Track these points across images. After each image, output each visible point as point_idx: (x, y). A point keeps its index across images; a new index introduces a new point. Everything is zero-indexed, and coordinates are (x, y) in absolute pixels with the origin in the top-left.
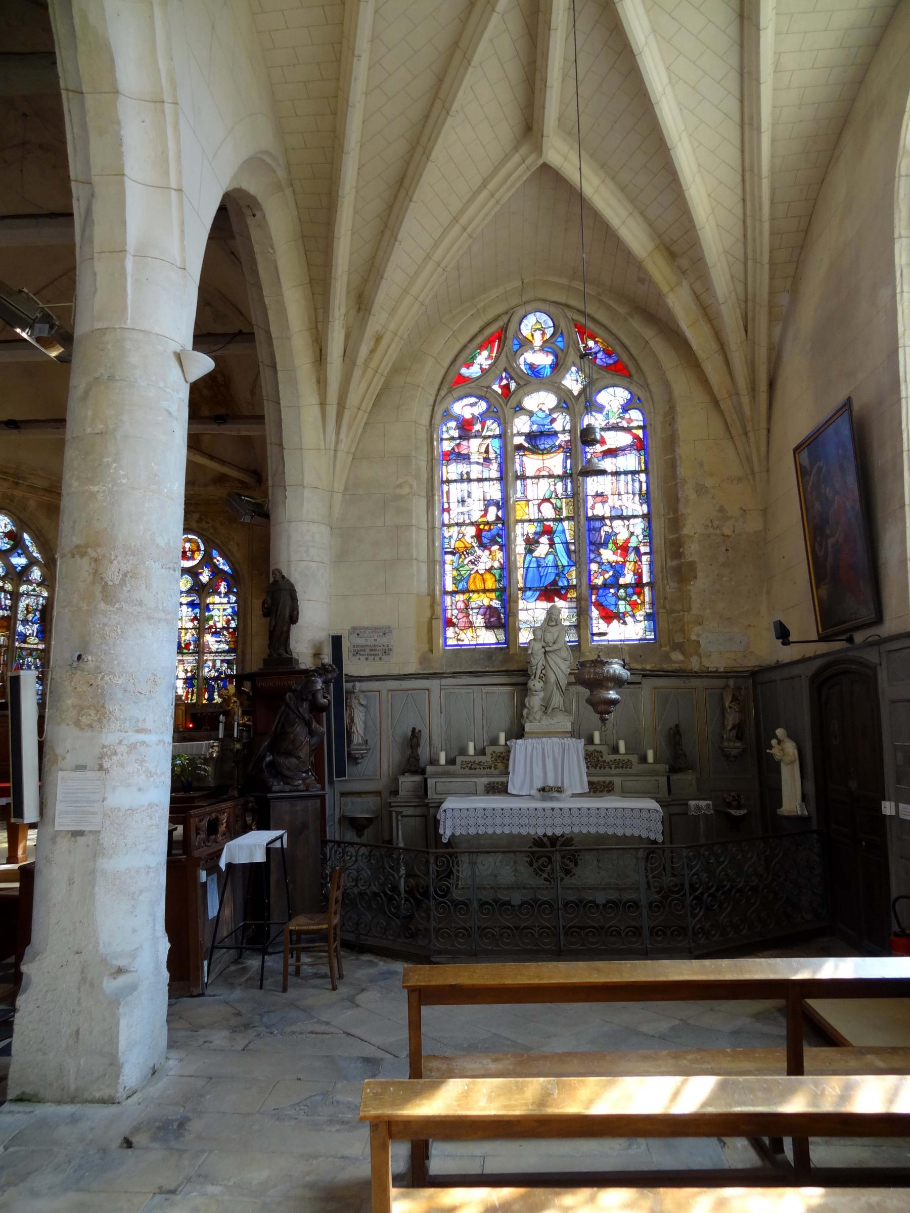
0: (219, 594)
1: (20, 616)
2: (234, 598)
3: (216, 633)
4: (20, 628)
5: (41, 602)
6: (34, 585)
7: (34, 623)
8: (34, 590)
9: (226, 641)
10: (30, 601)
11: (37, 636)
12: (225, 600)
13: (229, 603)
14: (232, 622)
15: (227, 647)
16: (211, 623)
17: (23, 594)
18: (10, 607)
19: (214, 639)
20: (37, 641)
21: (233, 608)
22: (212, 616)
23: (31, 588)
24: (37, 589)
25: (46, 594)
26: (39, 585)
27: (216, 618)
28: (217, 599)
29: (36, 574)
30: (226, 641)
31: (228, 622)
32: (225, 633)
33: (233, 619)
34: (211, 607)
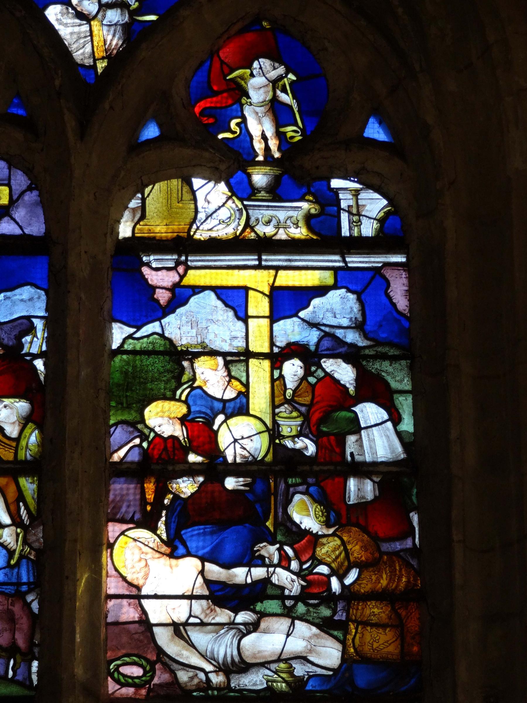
0: (232, 163)
2: (375, 204)
3: (226, 516)
9: (314, 592)
12: (289, 219)
13: (325, 237)
14: (370, 412)
15: (329, 654)
16: (163, 418)
19: (186, 574)
21: (366, 286)
22: (177, 358)
27: (211, 377)
28: (214, 206)
30: (314, 592)
31: (326, 412)
32: (305, 516)
33: (373, 388)
34: (159, 274)
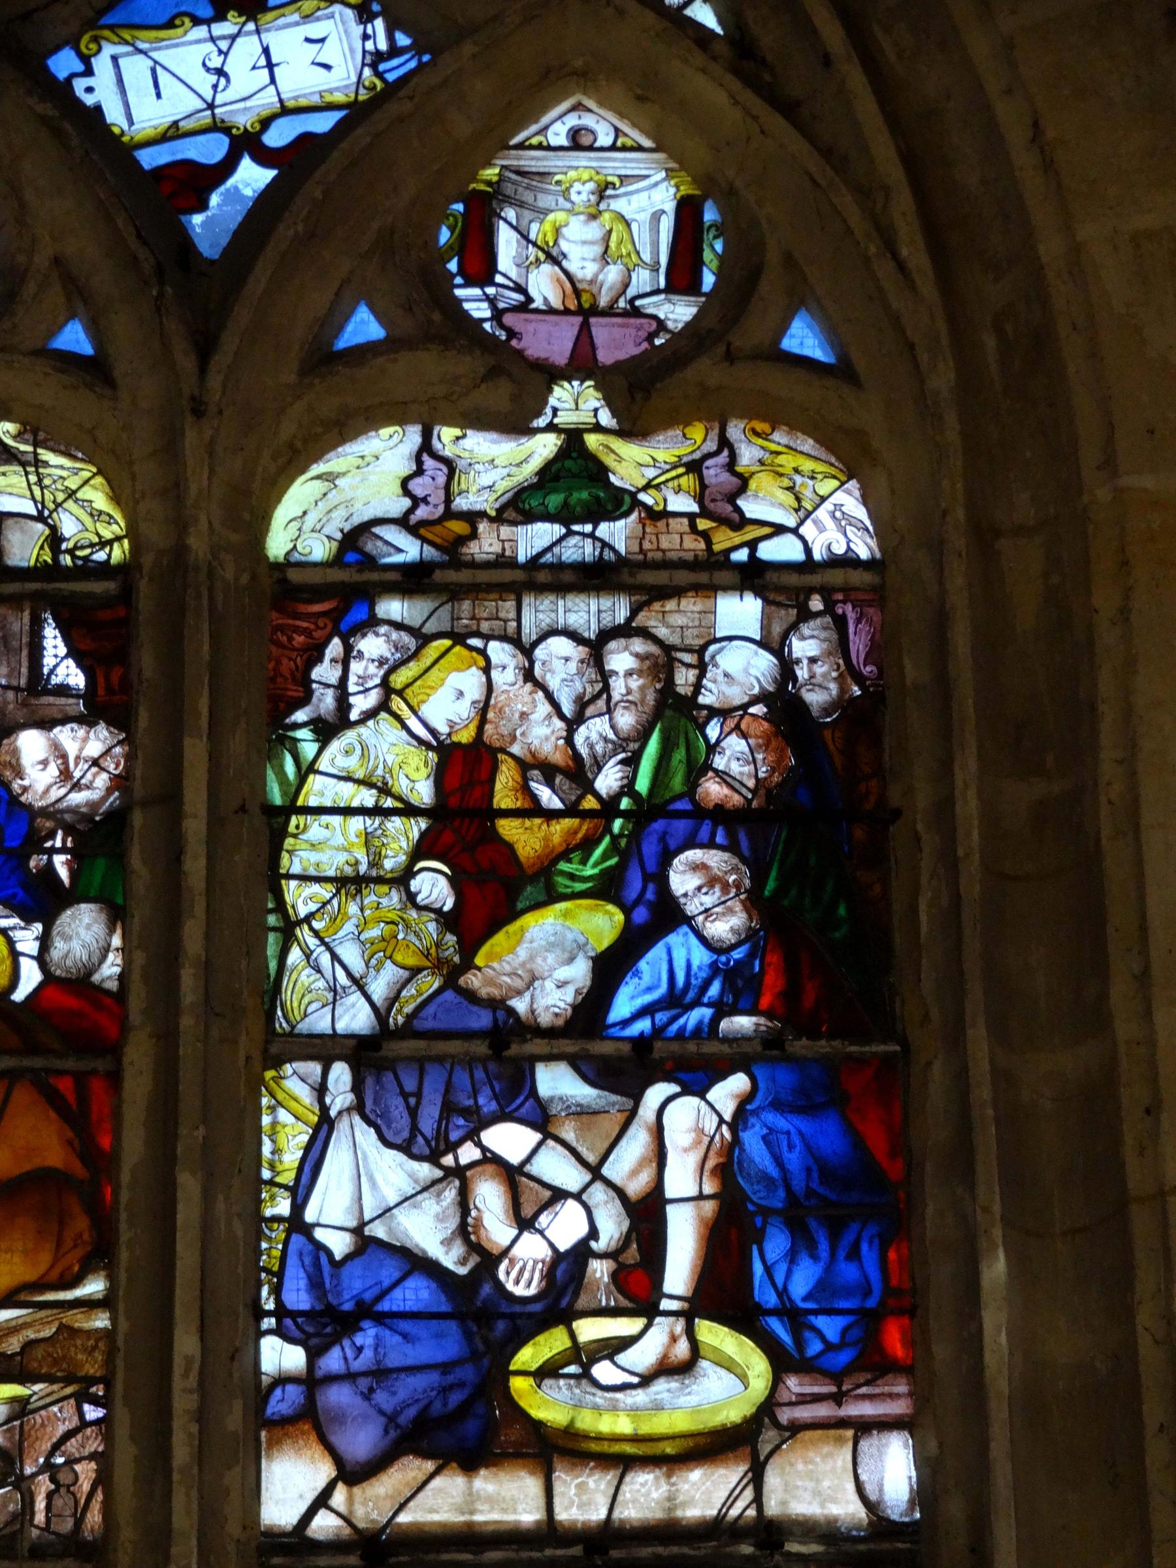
1: (339, 976)
4: (362, 1186)
5: (741, 670)
6: (575, 402)
7: (625, 1070)
8: (574, 483)
10: (539, 688)
11: (723, 1294)
17: (351, 583)
18: (97, 835)
20: (731, 1379)
23: (495, 463)
24: (630, 463)
25: (836, 522)
26: (643, 392)
29: (596, 214)
